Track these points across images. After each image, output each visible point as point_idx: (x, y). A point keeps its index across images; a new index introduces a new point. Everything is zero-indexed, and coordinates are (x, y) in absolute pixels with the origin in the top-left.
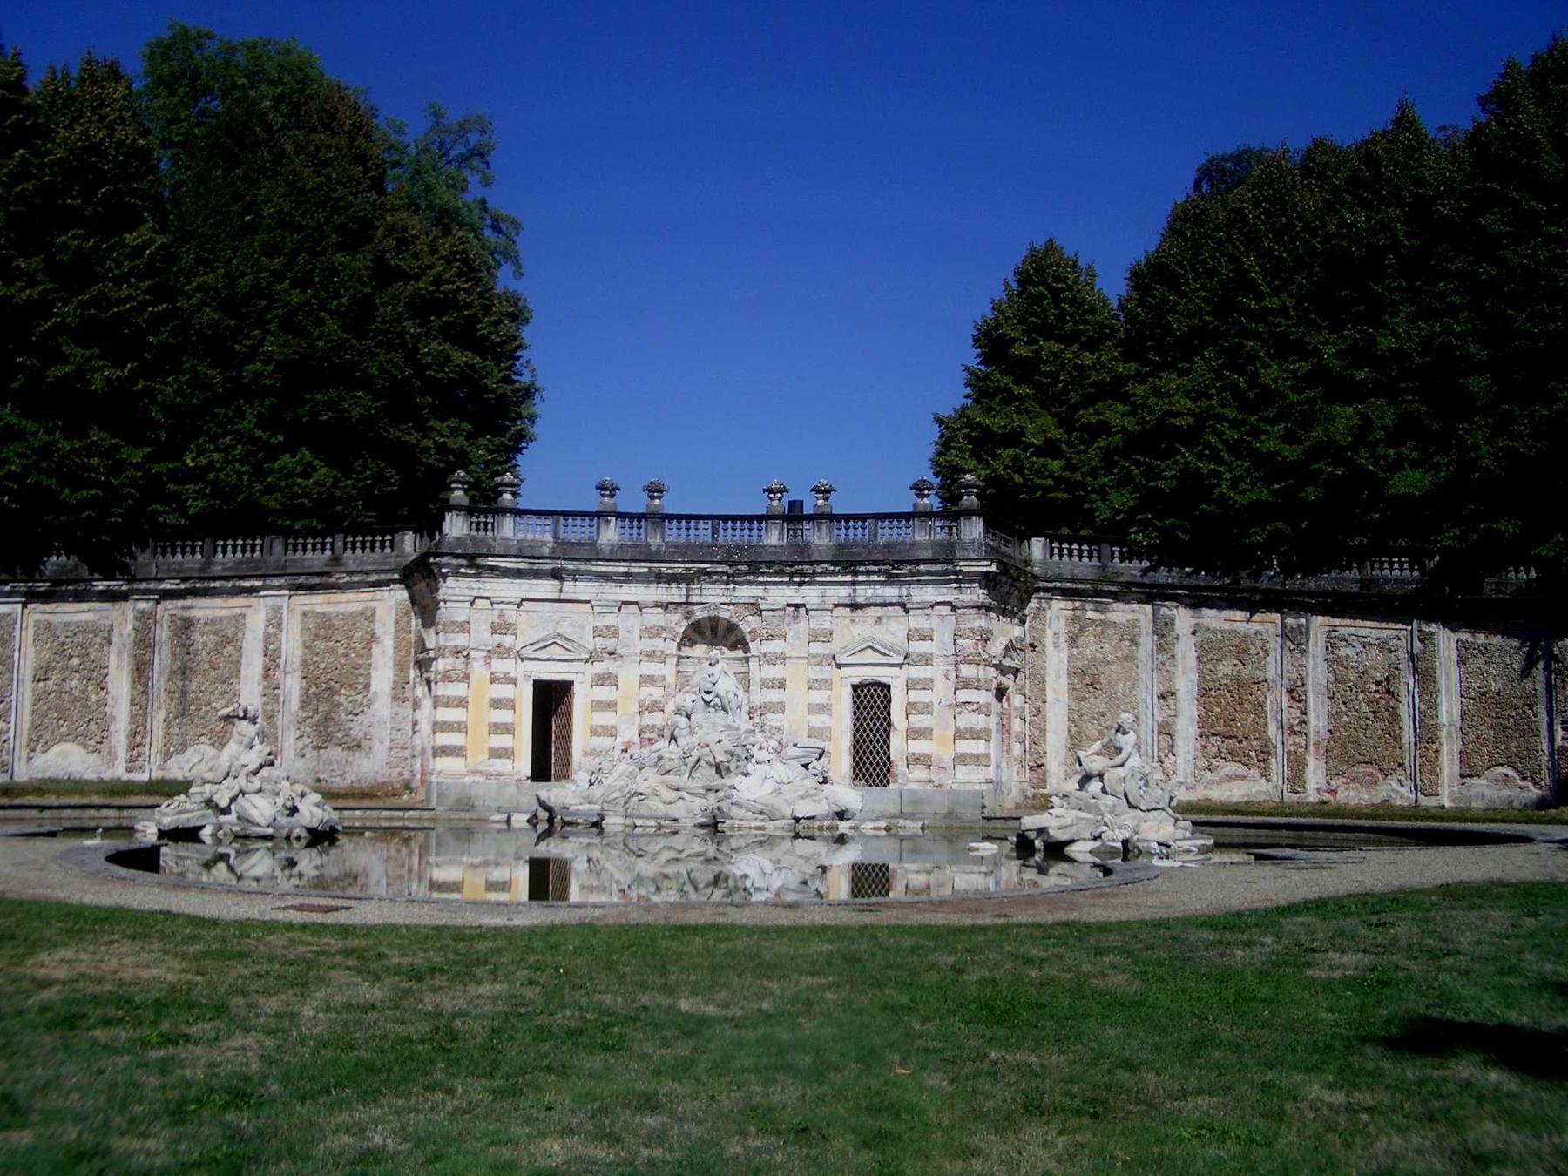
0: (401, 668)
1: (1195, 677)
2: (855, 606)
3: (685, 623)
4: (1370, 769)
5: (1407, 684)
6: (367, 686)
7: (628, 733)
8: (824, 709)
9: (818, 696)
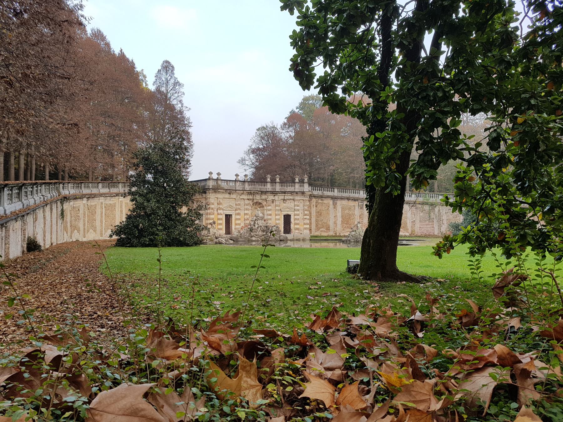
2: (284, 200)
7: (243, 225)
8: (279, 219)
9: (277, 217)
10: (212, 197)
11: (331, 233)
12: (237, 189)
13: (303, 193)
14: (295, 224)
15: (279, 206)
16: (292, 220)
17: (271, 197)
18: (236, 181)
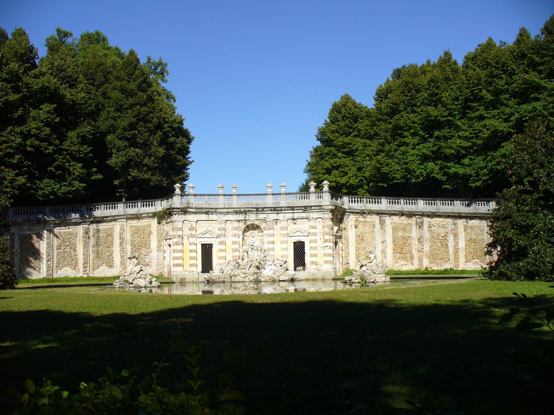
0: (159, 241)
1: (392, 237)
2: (294, 219)
3: (244, 226)
4: (440, 261)
5: (451, 238)
6: (150, 247)
9: (284, 246)
13: (320, 208)
14: (312, 255)
17: (273, 216)
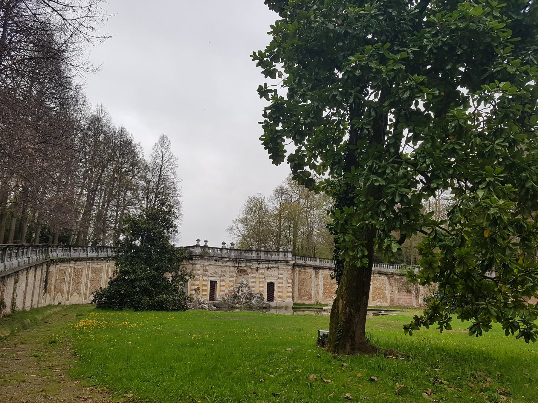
7: (227, 291)
8: (262, 287)
9: (261, 285)
10: (199, 264)
11: (313, 302)
12: (223, 256)
13: (287, 262)
14: (279, 292)
15: (263, 274)
16: (276, 288)
17: (255, 265)
18: (222, 249)
